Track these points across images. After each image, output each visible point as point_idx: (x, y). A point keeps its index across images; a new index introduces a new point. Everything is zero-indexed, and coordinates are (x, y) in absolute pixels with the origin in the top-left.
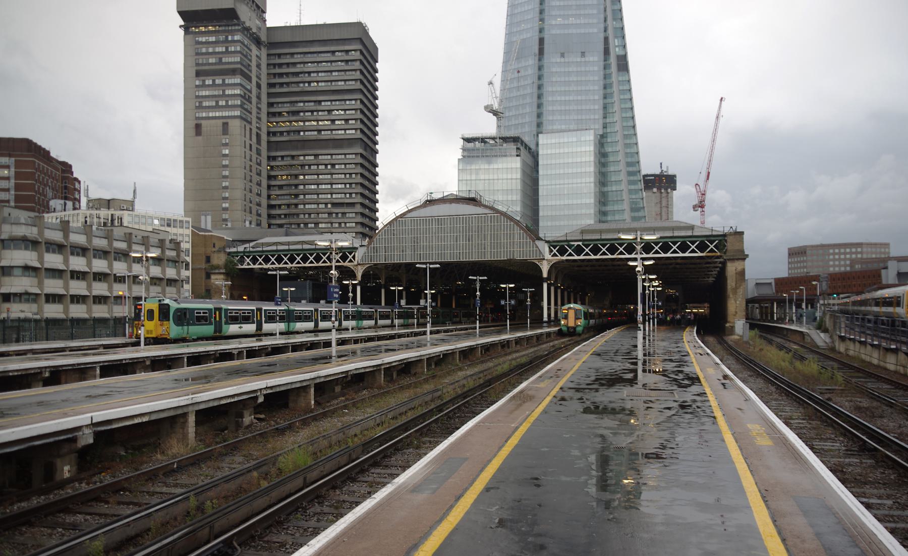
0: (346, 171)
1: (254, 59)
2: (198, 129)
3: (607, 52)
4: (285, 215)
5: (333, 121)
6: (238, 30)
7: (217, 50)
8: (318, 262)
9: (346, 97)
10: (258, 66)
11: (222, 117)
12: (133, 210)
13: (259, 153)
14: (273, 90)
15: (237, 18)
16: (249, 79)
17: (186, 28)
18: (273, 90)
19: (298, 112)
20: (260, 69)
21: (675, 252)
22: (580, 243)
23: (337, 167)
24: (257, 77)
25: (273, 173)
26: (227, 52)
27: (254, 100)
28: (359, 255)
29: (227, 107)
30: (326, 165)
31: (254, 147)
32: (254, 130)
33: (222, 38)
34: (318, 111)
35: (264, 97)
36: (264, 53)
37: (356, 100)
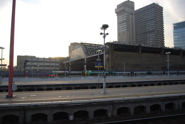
2: (120, 34)
5: (149, 27)
15: (125, 10)
26: (124, 18)
29: (125, 29)
32: (131, 32)
36: (134, 16)
37: (154, 21)
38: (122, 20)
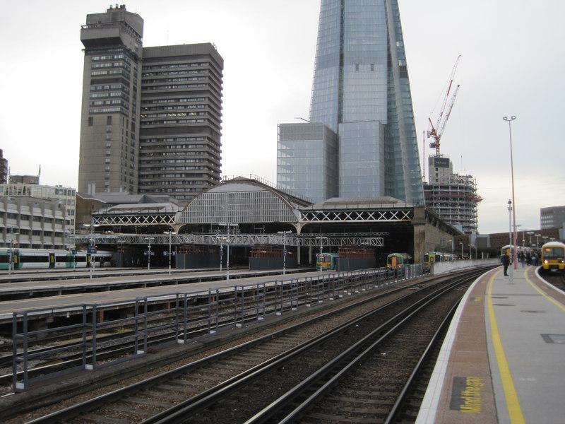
0: (196, 150)
1: (132, 70)
3: (389, 64)
4: (151, 182)
6: (122, 52)
7: (106, 65)
8: (150, 222)
9: (198, 96)
10: (135, 75)
11: (106, 113)
12: (38, 184)
13: (133, 137)
14: (145, 92)
16: (128, 85)
17: (87, 52)
18: (145, 92)
19: (163, 107)
20: (136, 77)
21: (383, 218)
22: (322, 212)
23: (190, 147)
24: (134, 83)
25: (143, 152)
26: (113, 67)
27: (131, 99)
28: (177, 217)
30: (182, 146)
31: (129, 134)
32: (130, 121)
33: (110, 57)
34: (177, 106)
35: (139, 98)
38: (105, 73)
